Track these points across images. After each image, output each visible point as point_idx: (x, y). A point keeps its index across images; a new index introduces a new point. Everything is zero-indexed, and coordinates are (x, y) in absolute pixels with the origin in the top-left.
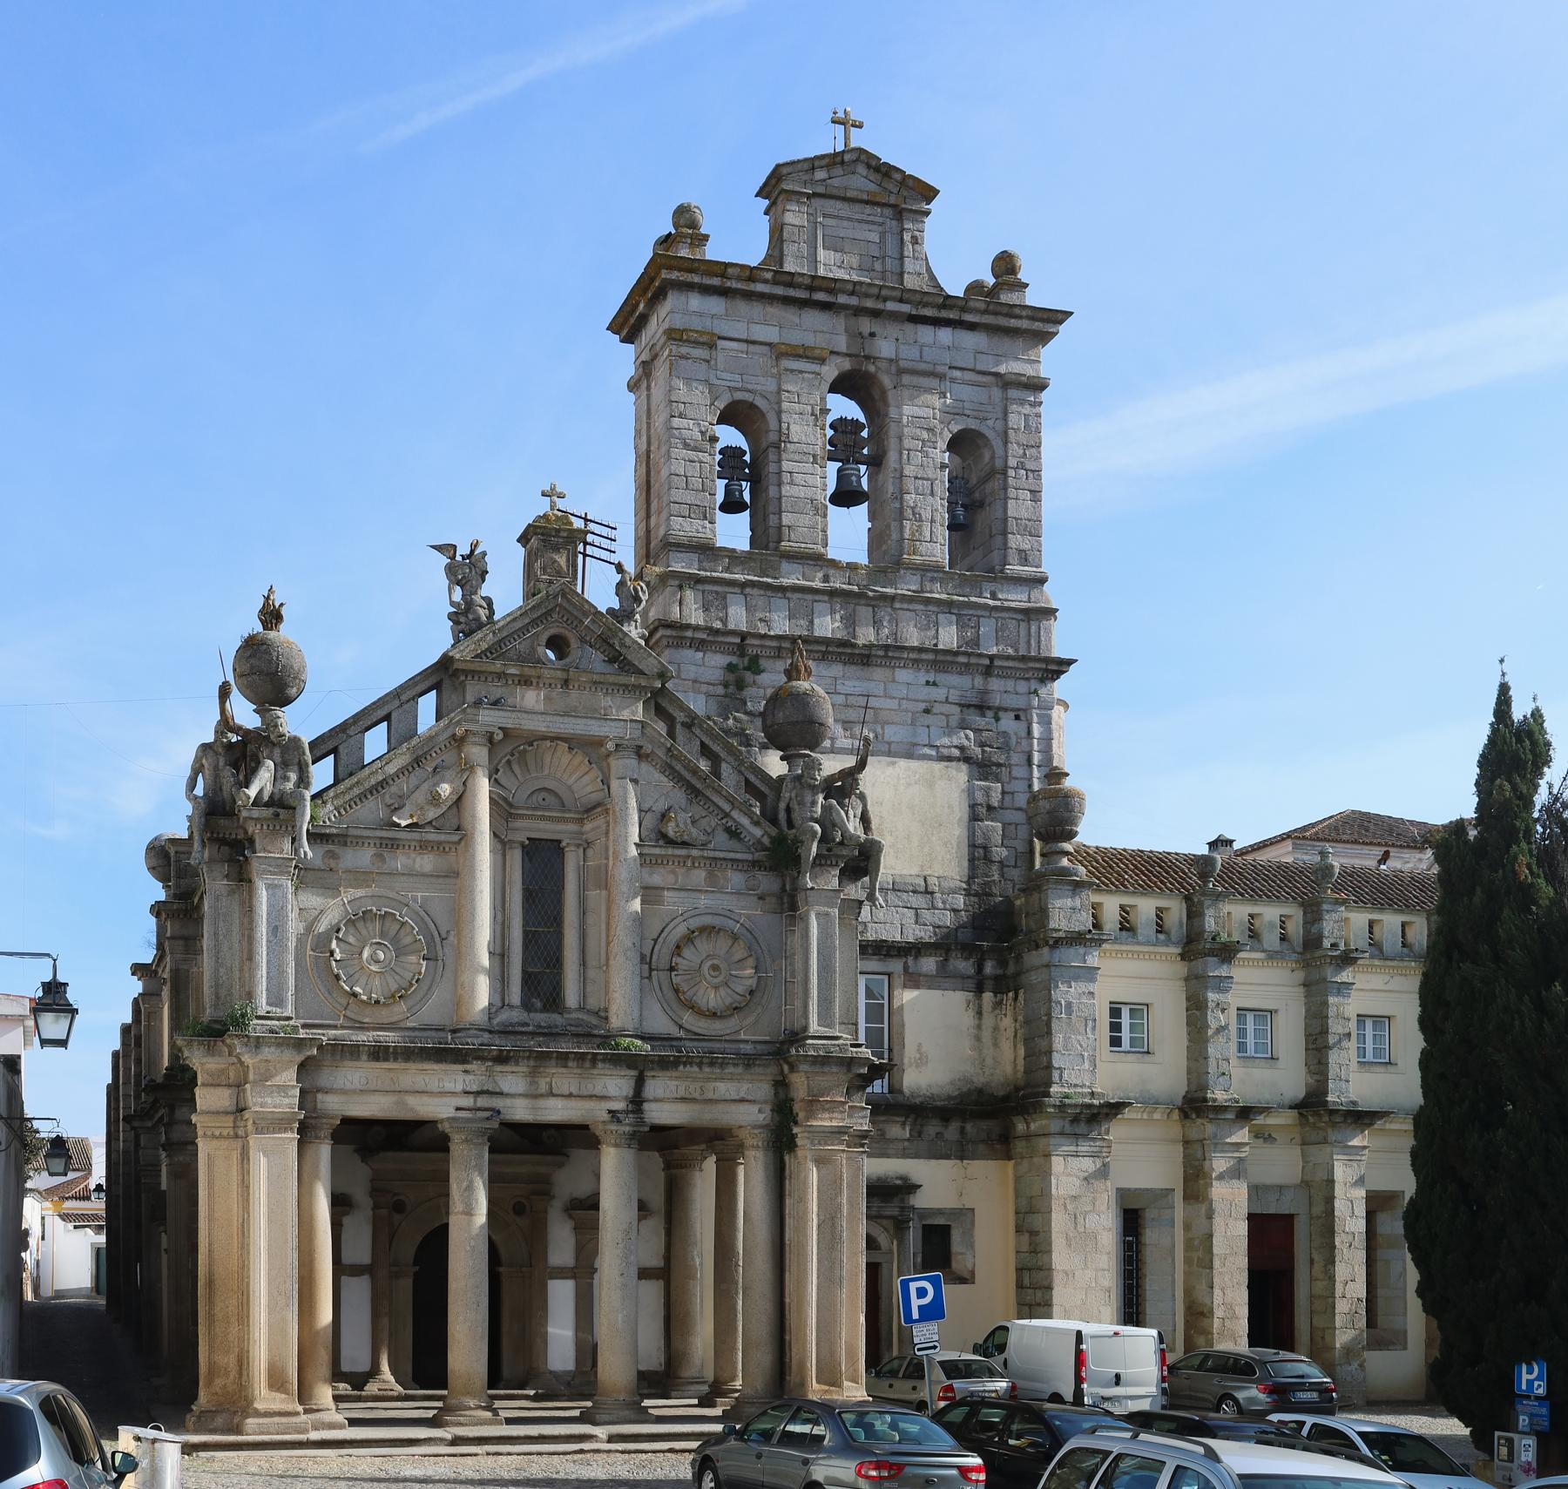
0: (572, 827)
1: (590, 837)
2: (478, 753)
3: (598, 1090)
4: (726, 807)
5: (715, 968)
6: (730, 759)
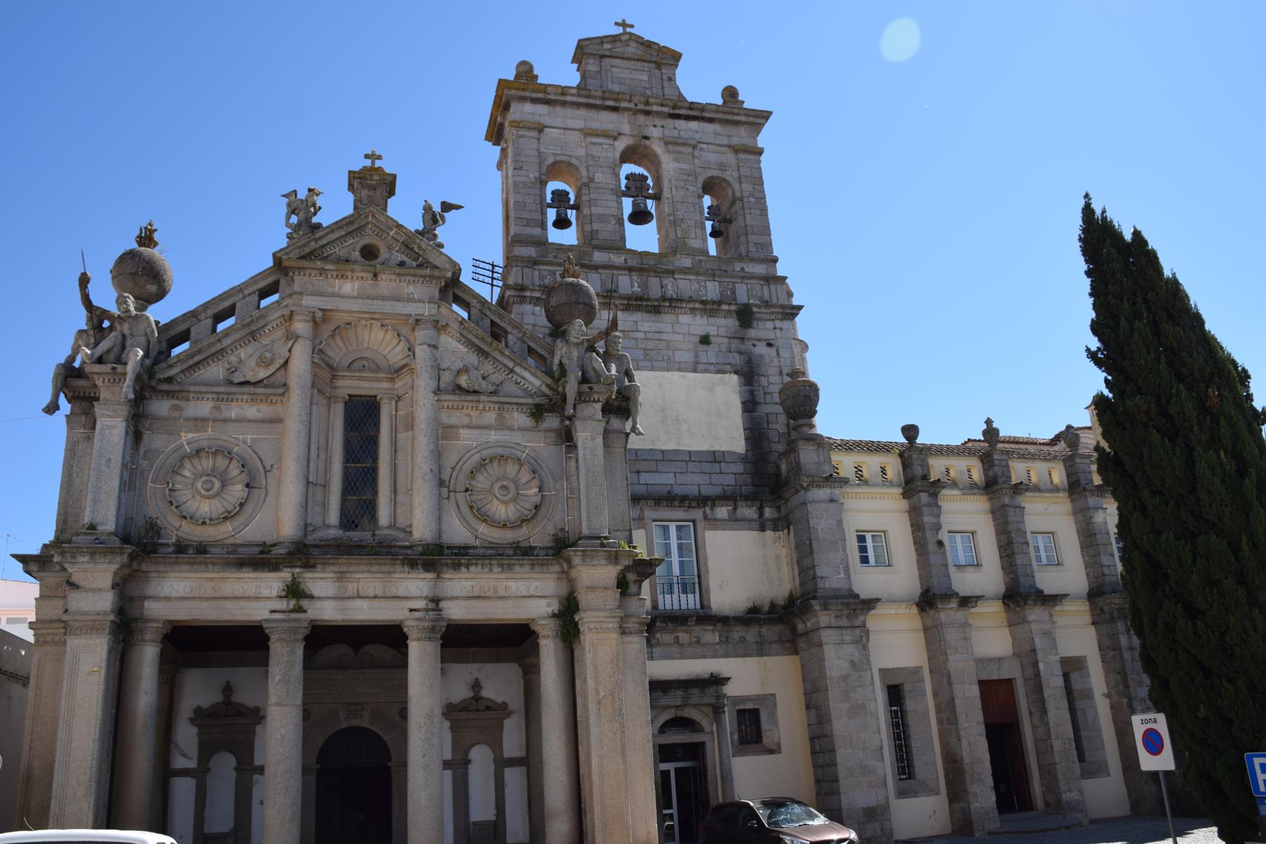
0: (386, 385)
1: (400, 392)
2: (301, 326)
3: (401, 592)
4: (511, 365)
5: (504, 487)
6: (515, 332)
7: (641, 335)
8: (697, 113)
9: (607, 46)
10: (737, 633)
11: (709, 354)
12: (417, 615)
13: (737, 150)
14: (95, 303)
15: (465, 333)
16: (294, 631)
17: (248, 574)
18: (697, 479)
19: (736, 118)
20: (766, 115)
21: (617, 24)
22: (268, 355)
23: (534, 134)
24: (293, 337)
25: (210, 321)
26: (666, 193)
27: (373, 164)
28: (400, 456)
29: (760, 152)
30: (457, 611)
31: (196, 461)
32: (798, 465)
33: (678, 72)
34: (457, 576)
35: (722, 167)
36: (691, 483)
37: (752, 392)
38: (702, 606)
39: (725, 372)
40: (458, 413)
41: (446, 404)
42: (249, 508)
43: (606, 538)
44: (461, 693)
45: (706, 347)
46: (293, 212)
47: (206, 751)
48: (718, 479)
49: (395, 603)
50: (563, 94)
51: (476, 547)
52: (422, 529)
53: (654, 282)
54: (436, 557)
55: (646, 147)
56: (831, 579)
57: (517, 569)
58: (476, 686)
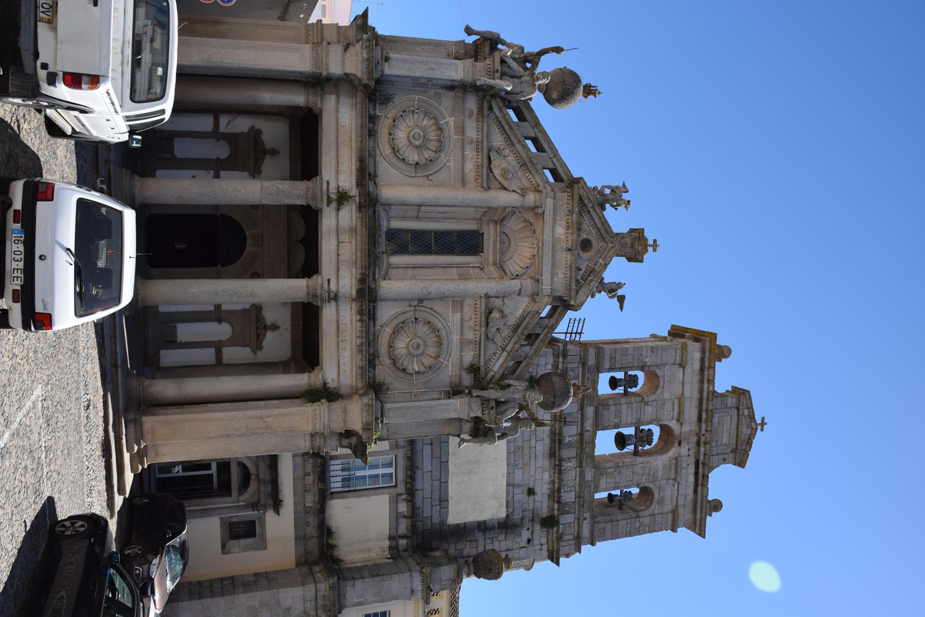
0: (491, 259)
1: (486, 269)
2: (531, 198)
3: (342, 273)
4: (508, 349)
6: (532, 352)
7: (533, 444)
8: (701, 481)
9: (746, 412)
10: (313, 520)
11: (520, 495)
12: (326, 285)
13: (674, 512)
14: (543, 57)
15: (530, 315)
16: (314, 198)
17: (354, 165)
18: (427, 487)
19: (699, 511)
20: (702, 533)
21: (763, 419)
22: (510, 176)
23: (678, 360)
24: (523, 193)
25: (533, 135)
26: (640, 459)
27: (650, 246)
28: (440, 271)
29: (674, 530)
30: (328, 313)
31: (434, 128)
32: (439, 565)
33: (731, 465)
34: (354, 312)
35: (661, 501)
36: (425, 484)
37: (493, 528)
38: (332, 493)
39: (507, 508)
40: (472, 311)
41: (478, 302)
42: (401, 165)
43: (382, 421)
44: (269, 316)
45: (526, 493)
46: (612, 190)
47: (231, 138)
48: (427, 503)
49: (334, 269)
50: (709, 381)
51: (374, 326)
52: (387, 287)
53: (572, 452)
54: (367, 297)
55: (672, 444)
56: (354, 591)
57: (359, 357)
58: (275, 327)
